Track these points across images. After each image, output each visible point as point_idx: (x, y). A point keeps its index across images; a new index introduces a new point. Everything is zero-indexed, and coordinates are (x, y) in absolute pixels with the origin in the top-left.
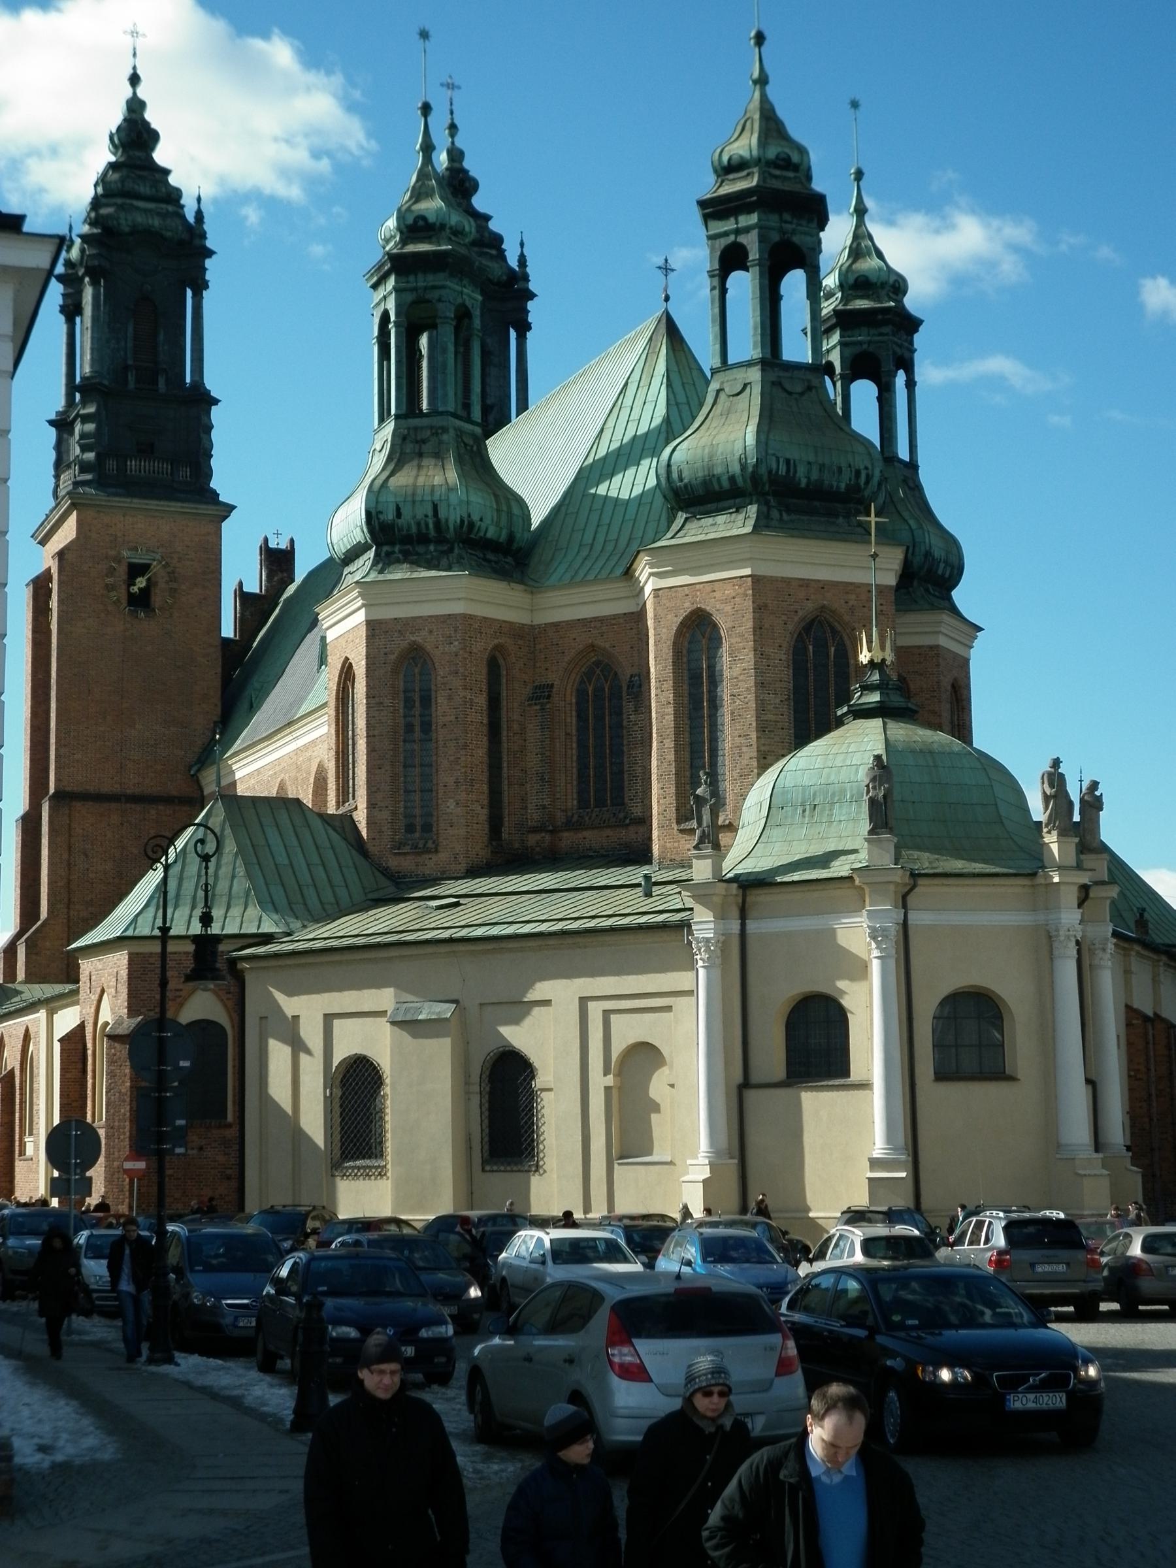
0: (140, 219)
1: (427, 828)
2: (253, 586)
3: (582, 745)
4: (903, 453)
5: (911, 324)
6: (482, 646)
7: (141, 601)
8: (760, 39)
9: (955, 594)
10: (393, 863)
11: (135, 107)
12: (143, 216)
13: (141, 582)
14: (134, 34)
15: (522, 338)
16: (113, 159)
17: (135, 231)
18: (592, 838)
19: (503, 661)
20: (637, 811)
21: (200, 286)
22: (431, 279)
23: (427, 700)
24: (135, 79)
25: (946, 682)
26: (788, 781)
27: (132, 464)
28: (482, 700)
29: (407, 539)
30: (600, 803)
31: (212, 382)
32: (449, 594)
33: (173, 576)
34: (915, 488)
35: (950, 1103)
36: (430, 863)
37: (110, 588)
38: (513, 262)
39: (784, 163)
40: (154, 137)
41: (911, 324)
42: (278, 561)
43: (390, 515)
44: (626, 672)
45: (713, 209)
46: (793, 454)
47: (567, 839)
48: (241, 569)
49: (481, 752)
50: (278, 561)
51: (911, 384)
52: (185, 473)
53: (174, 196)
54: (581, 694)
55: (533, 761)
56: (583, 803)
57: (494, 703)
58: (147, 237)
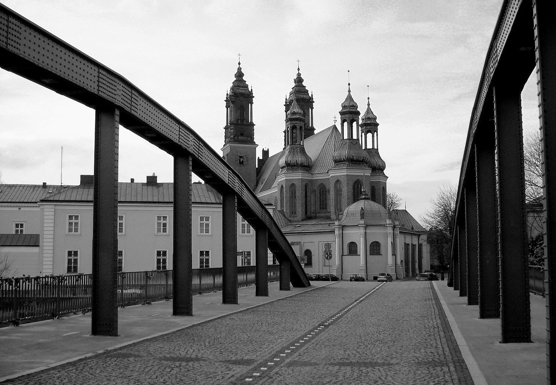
0: (241, 91)
1: (295, 213)
2: (261, 158)
3: (320, 199)
4: (376, 148)
5: (377, 125)
6: (304, 183)
7: (241, 163)
8: (349, 84)
9: (385, 172)
10: (290, 218)
11: (239, 69)
12: (241, 91)
13: (242, 159)
14: (239, 55)
15: (312, 110)
16: (235, 79)
17: (240, 93)
18: (322, 215)
19: (307, 185)
20: (329, 210)
21: (252, 103)
22: (296, 122)
23: (295, 192)
24: (239, 64)
25: (382, 187)
26: (350, 210)
27: (240, 137)
28: (304, 192)
29: (292, 166)
30: (323, 209)
31: (254, 121)
32: (298, 176)
33: (247, 158)
34: (378, 153)
35: (371, 258)
36: (296, 219)
37: (236, 161)
38: (310, 96)
39: (353, 106)
40: (243, 75)
41: (377, 125)
42: (266, 153)
43: (289, 162)
44: (327, 188)
45: (342, 113)
46: (354, 155)
47: (318, 215)
48: (259, 155)
49: (304, 201)
50: (266, 153)
51: (377, 135)
52: (249, 139)
53: (247, 86)
54: (320, 190)
55: (312, 202)
56: (320, 209)
57: (306, 192)
58: (242, 95)
